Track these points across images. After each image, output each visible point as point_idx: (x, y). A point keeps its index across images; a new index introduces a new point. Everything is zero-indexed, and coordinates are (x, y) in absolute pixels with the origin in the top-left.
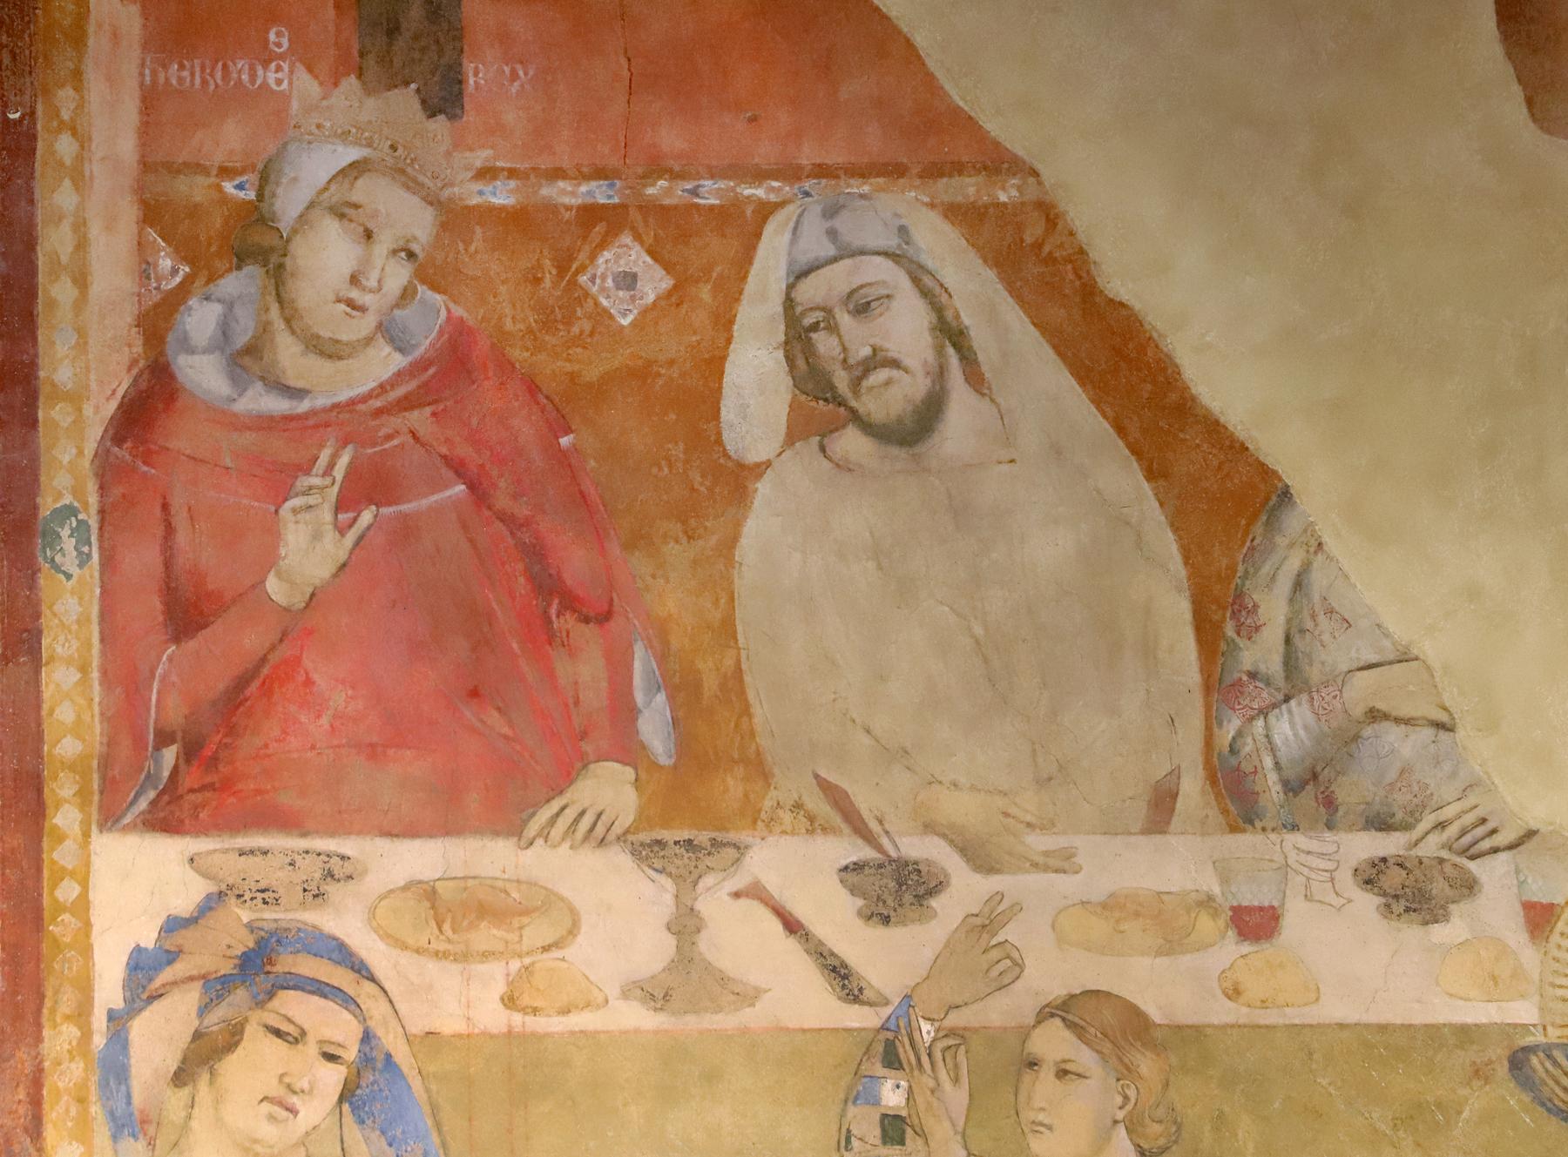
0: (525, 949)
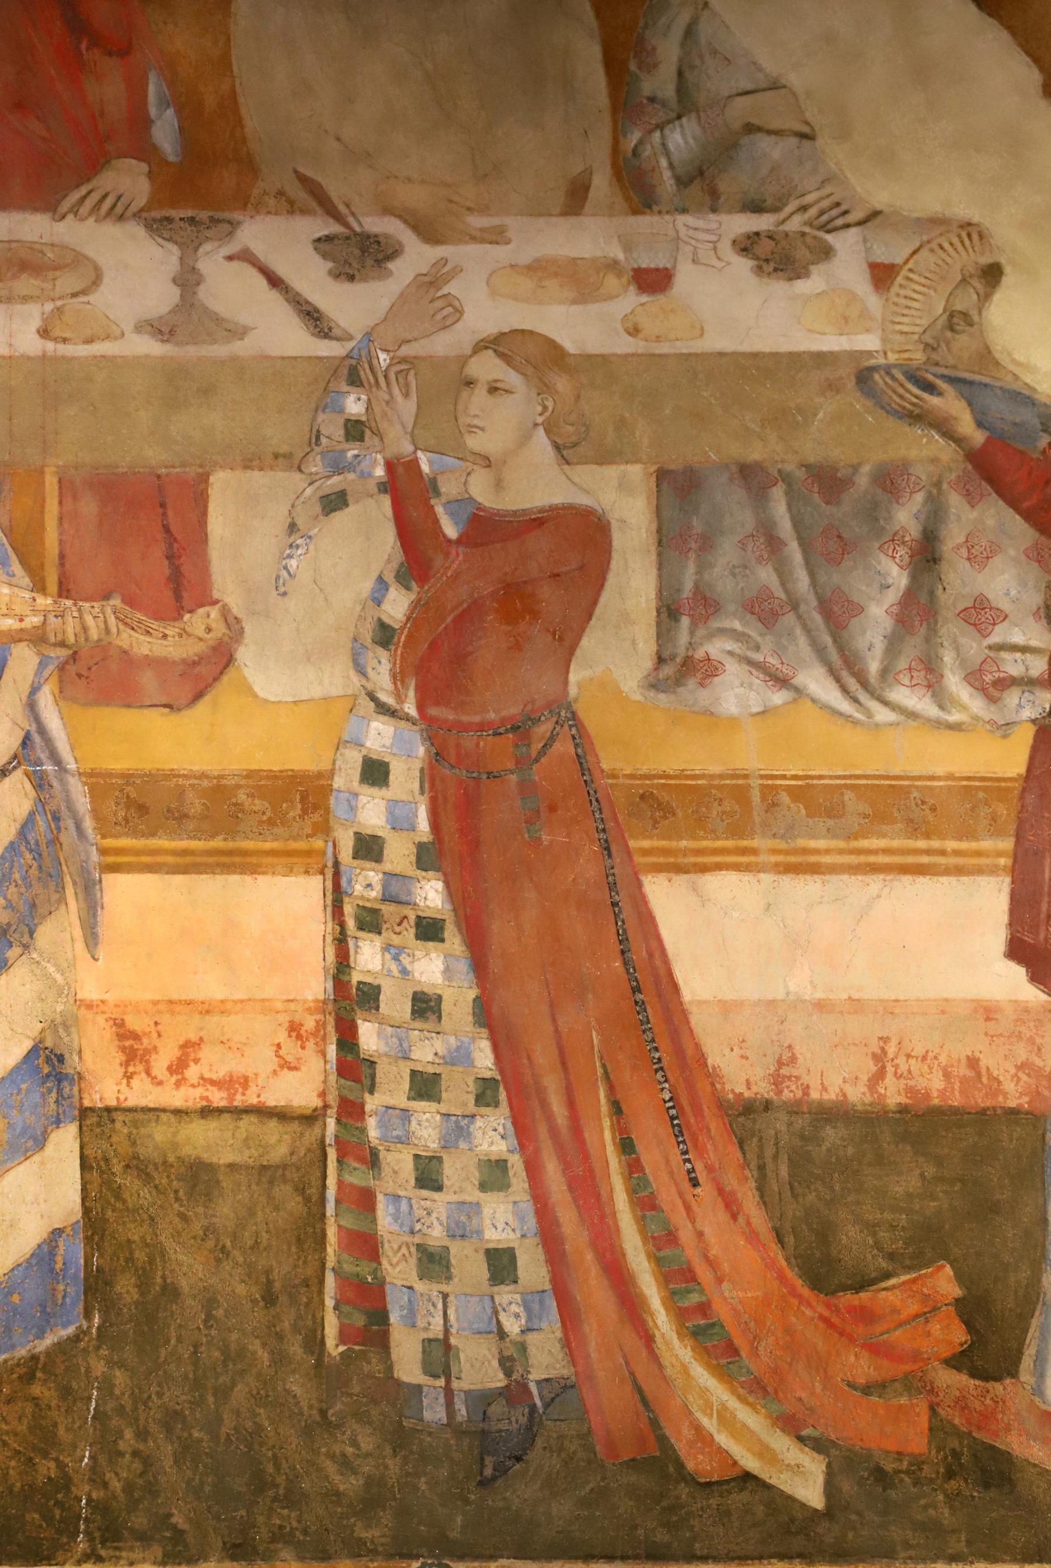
0: (57, 295)
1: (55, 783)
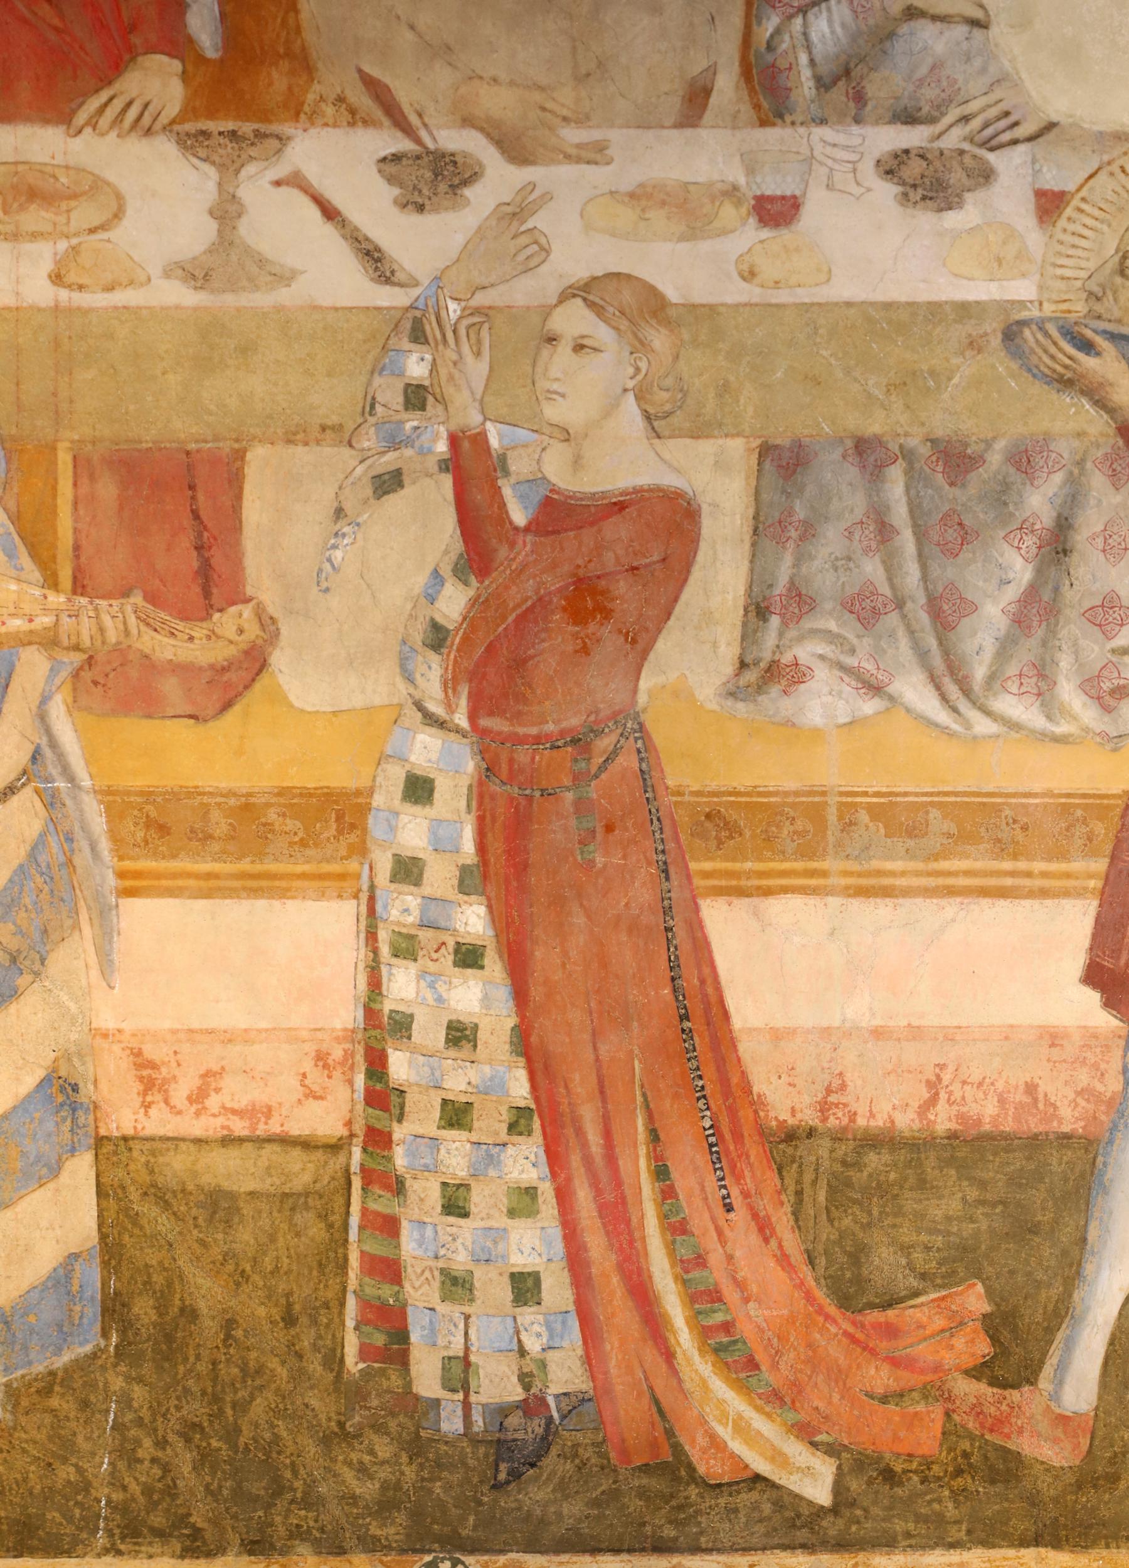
0: (72, 230)
1: (68, 802)
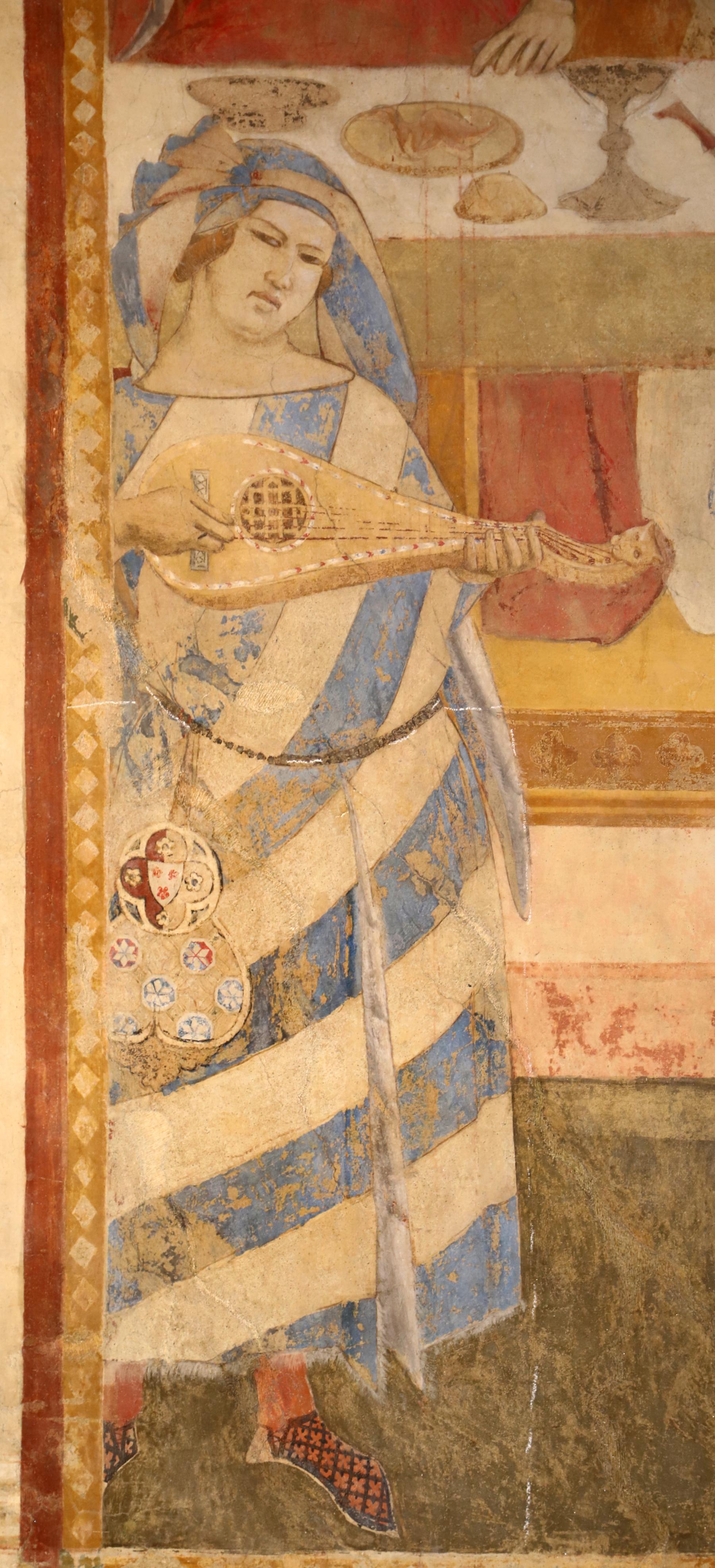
0: (475, 165)
1: (479, 726)
